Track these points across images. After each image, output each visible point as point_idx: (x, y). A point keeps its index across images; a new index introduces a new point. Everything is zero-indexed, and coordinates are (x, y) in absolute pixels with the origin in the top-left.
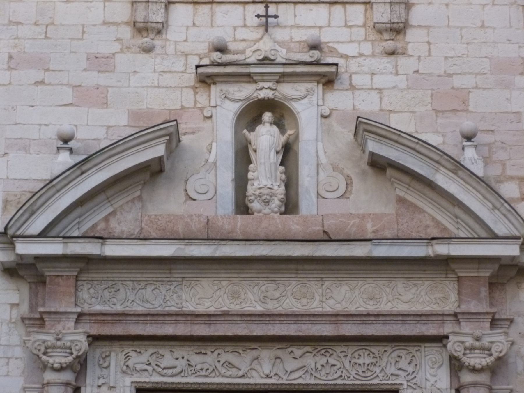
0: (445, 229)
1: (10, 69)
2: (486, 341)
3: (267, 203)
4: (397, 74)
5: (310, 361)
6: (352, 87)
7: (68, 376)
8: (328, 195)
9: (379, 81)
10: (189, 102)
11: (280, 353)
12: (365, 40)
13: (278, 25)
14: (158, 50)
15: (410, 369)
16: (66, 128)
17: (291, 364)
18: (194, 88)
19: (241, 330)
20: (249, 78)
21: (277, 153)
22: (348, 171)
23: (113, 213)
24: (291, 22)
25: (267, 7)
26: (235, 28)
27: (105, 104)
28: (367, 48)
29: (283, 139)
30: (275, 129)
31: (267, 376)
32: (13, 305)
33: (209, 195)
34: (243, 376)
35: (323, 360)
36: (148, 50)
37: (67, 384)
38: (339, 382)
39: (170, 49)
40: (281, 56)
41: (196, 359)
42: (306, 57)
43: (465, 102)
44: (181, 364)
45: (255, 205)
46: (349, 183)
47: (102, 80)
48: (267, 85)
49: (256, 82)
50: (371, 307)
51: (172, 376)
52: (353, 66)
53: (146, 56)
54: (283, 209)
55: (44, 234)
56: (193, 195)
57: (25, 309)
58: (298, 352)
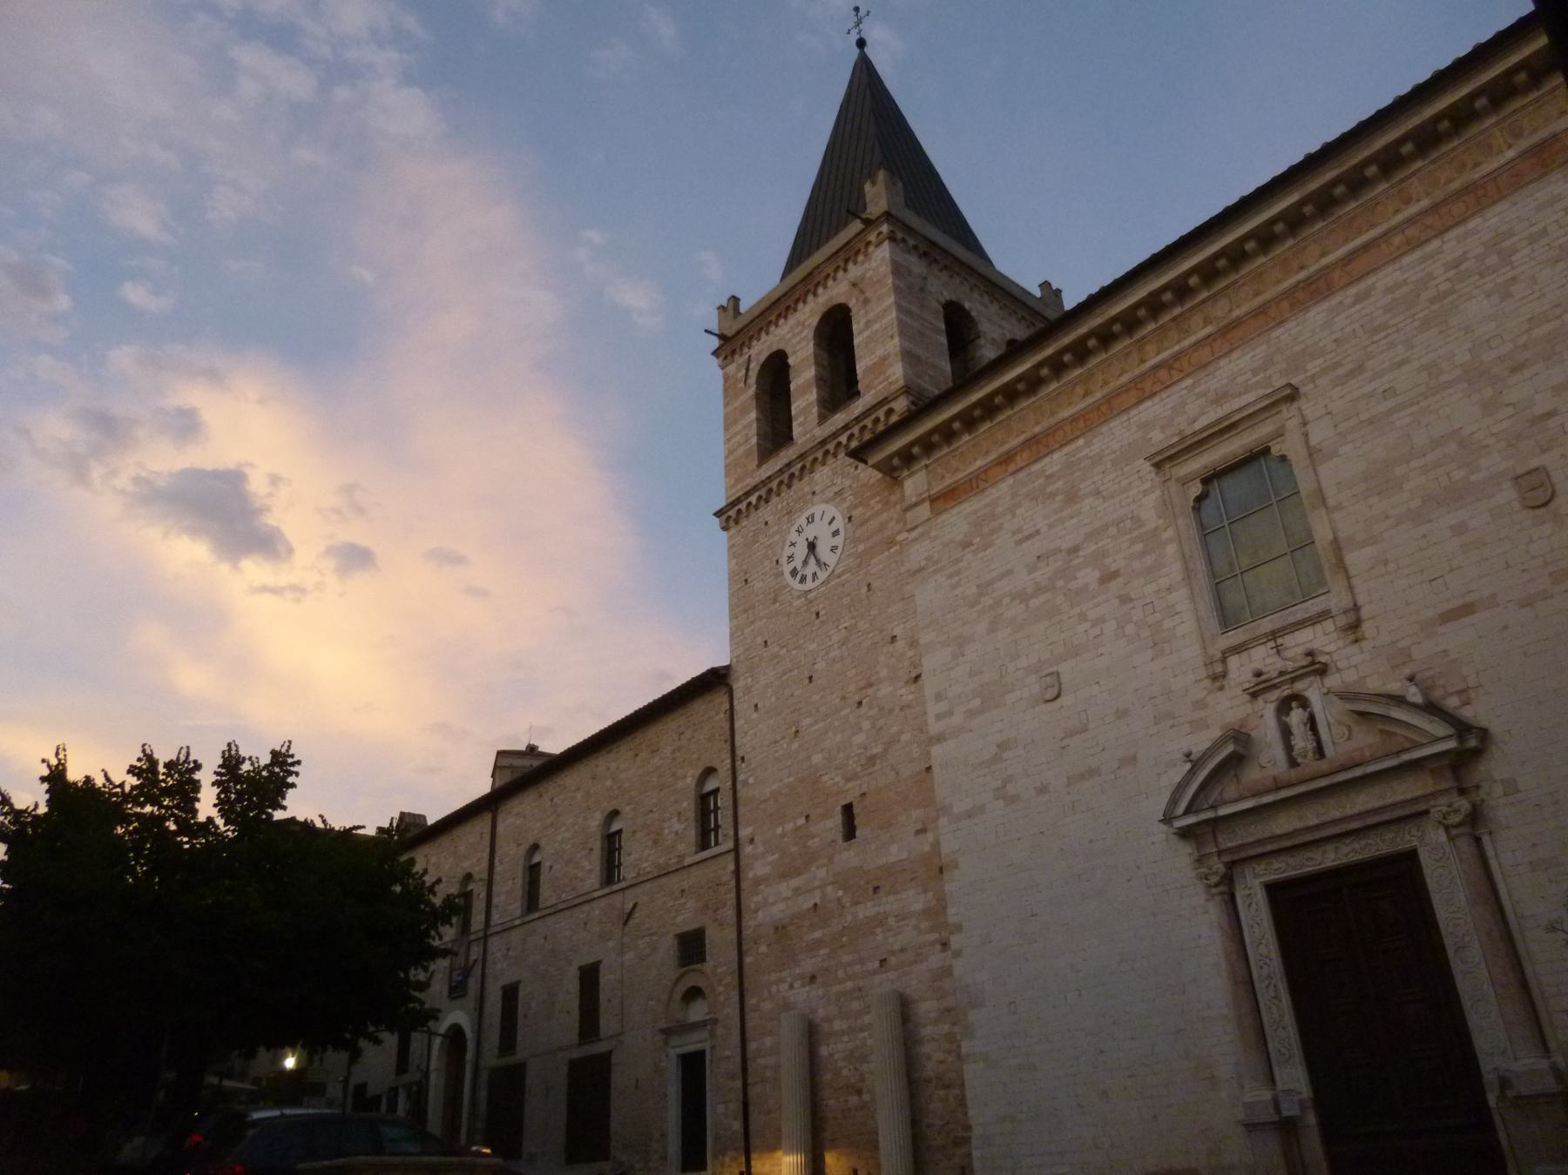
0: (1414, 741)
1: (1156, 724)
2: (1456, 806)
3: (1305, 757)
4: (1362, 653)
5: (1356, 845)
6: (1338, 670)
7: (1222, 888)
8: (1339, 741)
9: (1354, 661)
10: (1250, 711)
11: (1337, 845)
12: (1339, 638)
13: (1286, 648)
14: (1227, 687)
15: (1419, 834)
16: (1186, 750)
17: (1346, 849)
18: (1250, 702)
19: (1308, 837)
20: (1275, 687)
21: (1305, 724)
22: (1348, 723)
23: (1222, 790)
24: (1293, 644)
25: (1275, 642)
26: (1264, 659)
27: (1207, 727)
28: (1341, 643)
29: (1307, 714)
30: (1301, 710)
31: (1334, 861)
32: (1190, 855)
33: (1272, 762)
34: (1320, 864)
35: (1363, 842)
36: (1221, 688)
37: (1222, 893)
38: (1378, 853)
39: (1232, 683)
40: (1290, 665)
41: (1291, 861)
42: (1304, 663)
43: (1409, 655)
44: (1283, 865)
45: (1299, 760)
46: (1350, 729)
47: (1202, 714)
48: (1286, 687)
49: (1279, 687)
50: (1380, 803)
51: (1281, 873)
52: (1335, 657)
53: (1220, 692)
54: (1317, 757)
55: (1187, 812)
56: (1264, 765)
57: (1196, 854)
58: (1348, 841)
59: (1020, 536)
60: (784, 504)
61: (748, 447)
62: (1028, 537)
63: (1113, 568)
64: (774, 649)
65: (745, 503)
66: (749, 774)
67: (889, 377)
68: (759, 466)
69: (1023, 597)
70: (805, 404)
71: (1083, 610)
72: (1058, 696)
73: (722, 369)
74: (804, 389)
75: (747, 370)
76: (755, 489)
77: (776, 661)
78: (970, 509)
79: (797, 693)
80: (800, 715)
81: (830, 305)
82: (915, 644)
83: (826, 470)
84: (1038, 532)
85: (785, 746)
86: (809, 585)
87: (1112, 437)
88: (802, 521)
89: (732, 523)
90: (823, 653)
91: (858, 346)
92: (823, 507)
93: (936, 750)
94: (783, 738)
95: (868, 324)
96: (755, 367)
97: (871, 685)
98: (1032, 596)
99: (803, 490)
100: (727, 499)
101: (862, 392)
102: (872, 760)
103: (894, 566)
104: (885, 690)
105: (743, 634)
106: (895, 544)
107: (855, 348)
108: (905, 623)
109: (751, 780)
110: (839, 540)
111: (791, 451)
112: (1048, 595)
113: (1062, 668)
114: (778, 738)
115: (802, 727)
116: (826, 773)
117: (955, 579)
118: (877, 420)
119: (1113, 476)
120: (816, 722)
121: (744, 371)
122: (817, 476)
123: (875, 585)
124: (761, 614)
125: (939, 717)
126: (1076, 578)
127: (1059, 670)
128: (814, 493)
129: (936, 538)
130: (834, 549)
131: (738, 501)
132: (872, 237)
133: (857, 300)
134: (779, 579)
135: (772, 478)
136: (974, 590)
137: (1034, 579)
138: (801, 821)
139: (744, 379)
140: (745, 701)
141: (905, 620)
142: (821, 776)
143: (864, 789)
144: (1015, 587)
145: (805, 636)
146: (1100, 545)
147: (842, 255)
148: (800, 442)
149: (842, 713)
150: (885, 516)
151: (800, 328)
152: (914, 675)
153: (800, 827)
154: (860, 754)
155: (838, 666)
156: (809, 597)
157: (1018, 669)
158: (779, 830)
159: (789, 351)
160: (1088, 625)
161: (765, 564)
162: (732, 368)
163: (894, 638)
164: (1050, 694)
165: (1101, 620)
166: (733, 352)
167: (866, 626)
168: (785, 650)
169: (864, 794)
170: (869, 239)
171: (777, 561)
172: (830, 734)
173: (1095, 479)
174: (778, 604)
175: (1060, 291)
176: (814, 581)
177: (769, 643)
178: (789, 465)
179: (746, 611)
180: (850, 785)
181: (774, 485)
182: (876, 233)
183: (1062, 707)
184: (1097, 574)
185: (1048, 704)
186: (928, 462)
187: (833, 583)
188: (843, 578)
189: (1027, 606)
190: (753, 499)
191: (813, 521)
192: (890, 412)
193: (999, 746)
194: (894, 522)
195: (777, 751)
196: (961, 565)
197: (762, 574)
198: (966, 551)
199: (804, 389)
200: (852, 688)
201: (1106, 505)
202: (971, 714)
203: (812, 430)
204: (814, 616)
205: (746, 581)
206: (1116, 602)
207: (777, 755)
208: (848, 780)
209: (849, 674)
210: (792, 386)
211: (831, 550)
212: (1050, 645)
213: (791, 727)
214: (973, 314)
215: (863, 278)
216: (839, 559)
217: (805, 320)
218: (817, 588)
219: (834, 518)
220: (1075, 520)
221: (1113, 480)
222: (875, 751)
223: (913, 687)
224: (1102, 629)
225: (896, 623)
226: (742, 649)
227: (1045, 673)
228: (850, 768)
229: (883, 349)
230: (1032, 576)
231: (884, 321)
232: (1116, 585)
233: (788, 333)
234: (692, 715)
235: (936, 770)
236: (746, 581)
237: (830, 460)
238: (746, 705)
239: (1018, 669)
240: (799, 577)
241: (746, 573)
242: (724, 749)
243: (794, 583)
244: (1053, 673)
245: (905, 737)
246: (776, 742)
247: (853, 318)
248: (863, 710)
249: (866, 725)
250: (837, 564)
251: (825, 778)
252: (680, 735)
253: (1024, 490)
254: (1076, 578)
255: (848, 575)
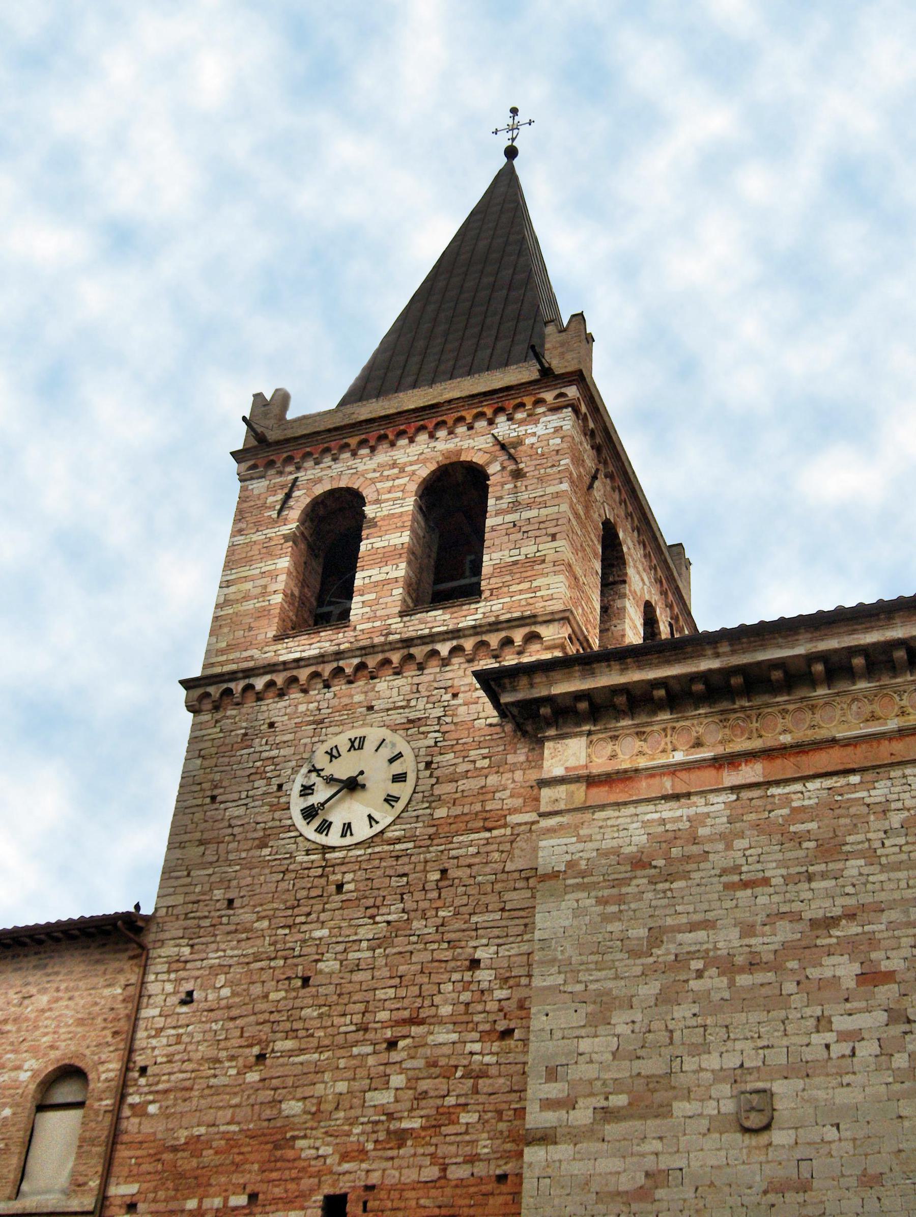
59: (736, 878)
60: (313, 706)
61: (267, 603)
62: (746, 885)
63: (885, 966)
64: (245, 916)
65: (242, 684)
66: (151, 1097)
67: (539, 588)
68: (278, 638)
69: (728, 967)
70: (383, 576)
71: (826, 1013)
72: (767, 1127)
73: (241, 481)
74: (385, 557)
75: (288, 496)
76: (271, 668)
77: (244, 936)
78: (656, 816)
79: (273, 996)
80: (274, 1032)
81: (454, 459)
82: (511, 982)
83: (399, 682)
84: (766, 882)
85: (233, 1072)
86: (333, 838)
87: (906, 788)
88: (342, 741)
89: (207, 705)
90: (340, 948)
91: (493, 529)
92: (385, 733)
93: (534, 1155)
94: (232, 1058)
95: (516, 506)
96: (301, 500)
97: (422, 1022)
98: (741, 970)
99: (351, 696)
100: (205, 667)
101: (486, 594)
102: (401, 1137)
103: (496, 856)
104: (444, 1036)
105: (188, 875)
106: (505, 826)
107: (487, 530)
108: (499, 945)
109: (152, 1109)
110: (404, 791)
111: (341, 635)
112: (770, 976)
113: (778, 1087)
114: (223, 1054)
115: (273, 1051)
116: (305, 1137)
117: (614, 908)
118: (508, 642)
119: (902, 841)
120: (302, 1051)
121: (280, 496)
122: (381, 685)
123: (452, 873)
124: (231, 857)
125: (548, 1104)
126: (821, 965)
127: (774, 1089)
128: (370, 708)
129: (590, 839)
130: (390, 800)
131: (232, 676)
132: (549, 396)
133: (503, 468)
134: (277, 815)
135: (302, 663)
136: (643, 932)
137: (750, 946)
138: (240, 1200)
139: (278, 507)
140: (169, 981)
141: (500, 941)
142: (294, 1138)
143: (374, 1178)
144: (716, 948)
145: (309, 914)
146: (867, 928)
147: (495, 402)
148: (359, 627)
149: (355, 1050)
150: (493, 780)
151: (396, 471)
152: (501, 1026)
153: (235, 1209)
154: (376, 1123)
155: (358, 977)
156: (327, 856)
157: (701, 1069)
158: (192, 1204)
159: (368, 493)
160: (830, 1037)
161: (256, 784)
162: (258, 486)
163: (475, 964)
164: (754, 1120)
165: (856, 1036)
166: (271, 464)
167: (426, 931)
168: (266, 923)
169: (370, 1188)
170: (543, 395)
171: (280, 787)
172: (327, 1076)
173: (870, 836)
174: (266, 851)
175: (690, 564)
176: (343, 835)
177: (237, 903)
178: (339, 655)
179: (201, 843)
180: (346, 1166)
181: (303, 674)
182: (556, 392)
183: (770, 1144)
184: (856, 968)
185: (747, 1135)
186: (593, 728)
187: (377, 849)
188: (398, 847)
189: (732, 984)
190: (259, 683)
191: (361, 747)
192: (532, 637)
193: (647, 1175)
194: (508, 793)
195: (215, 1076)
196: (624, 890)
197: (247, 797)
198: (639, 873)
199: (385, 557)
200: (383, 1016)
201: (883, 877)
202: (607, 1114)
203: (388, 617)
204: (333, 888)
205: (213, 798)
206: (883, 1017)
207: (213, 1081)
208: (345, 1157)
209: (380, 994)
210: (364, 546)
211: (386, 800)
212: (762, 1048)
213: (251, 1046)
214: (625, 549)
215: (519, 442)
216: (398, 817)
217: (405, 464)
218: (348, 848)
219: (400, 755)
220: (831, 883)
221: (901, 846)
222: (405, 1124)
223: (495, 1048)
224: (853, 1049)
225: (484, 941)
226: (180, 899)
227: (749, 1087)
228: (353, 1139)
229: (534, 548)
230: (746, 941)
231: (544, 512)
232: (886, 993)
233: (374, 471)
234: (57, 973)
235: (528, 1186)
236: (213, 798)
237: (410, 671)
238: (169, 987)
239: (701, 1069)
240: (316, 823)
241: (216, 787)
242: (108, 1044)
243: (309, 831)
244: (764, 1091)
245: (465, 1118)
246: (217, 1060)
247: (490, 490)
248: (395, 1056)
249: (398, 1080)
250: (393, 823)
251: (300, 1143)
252: (24, 998)
253: (753, 816)
254: (821, 965)
255: (411, 845)
